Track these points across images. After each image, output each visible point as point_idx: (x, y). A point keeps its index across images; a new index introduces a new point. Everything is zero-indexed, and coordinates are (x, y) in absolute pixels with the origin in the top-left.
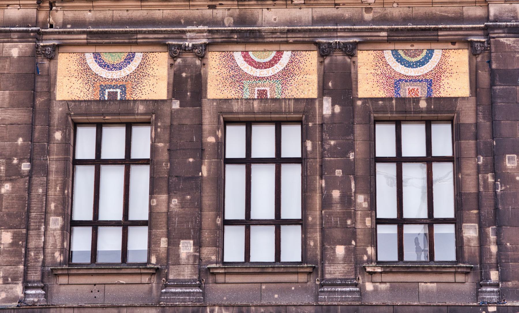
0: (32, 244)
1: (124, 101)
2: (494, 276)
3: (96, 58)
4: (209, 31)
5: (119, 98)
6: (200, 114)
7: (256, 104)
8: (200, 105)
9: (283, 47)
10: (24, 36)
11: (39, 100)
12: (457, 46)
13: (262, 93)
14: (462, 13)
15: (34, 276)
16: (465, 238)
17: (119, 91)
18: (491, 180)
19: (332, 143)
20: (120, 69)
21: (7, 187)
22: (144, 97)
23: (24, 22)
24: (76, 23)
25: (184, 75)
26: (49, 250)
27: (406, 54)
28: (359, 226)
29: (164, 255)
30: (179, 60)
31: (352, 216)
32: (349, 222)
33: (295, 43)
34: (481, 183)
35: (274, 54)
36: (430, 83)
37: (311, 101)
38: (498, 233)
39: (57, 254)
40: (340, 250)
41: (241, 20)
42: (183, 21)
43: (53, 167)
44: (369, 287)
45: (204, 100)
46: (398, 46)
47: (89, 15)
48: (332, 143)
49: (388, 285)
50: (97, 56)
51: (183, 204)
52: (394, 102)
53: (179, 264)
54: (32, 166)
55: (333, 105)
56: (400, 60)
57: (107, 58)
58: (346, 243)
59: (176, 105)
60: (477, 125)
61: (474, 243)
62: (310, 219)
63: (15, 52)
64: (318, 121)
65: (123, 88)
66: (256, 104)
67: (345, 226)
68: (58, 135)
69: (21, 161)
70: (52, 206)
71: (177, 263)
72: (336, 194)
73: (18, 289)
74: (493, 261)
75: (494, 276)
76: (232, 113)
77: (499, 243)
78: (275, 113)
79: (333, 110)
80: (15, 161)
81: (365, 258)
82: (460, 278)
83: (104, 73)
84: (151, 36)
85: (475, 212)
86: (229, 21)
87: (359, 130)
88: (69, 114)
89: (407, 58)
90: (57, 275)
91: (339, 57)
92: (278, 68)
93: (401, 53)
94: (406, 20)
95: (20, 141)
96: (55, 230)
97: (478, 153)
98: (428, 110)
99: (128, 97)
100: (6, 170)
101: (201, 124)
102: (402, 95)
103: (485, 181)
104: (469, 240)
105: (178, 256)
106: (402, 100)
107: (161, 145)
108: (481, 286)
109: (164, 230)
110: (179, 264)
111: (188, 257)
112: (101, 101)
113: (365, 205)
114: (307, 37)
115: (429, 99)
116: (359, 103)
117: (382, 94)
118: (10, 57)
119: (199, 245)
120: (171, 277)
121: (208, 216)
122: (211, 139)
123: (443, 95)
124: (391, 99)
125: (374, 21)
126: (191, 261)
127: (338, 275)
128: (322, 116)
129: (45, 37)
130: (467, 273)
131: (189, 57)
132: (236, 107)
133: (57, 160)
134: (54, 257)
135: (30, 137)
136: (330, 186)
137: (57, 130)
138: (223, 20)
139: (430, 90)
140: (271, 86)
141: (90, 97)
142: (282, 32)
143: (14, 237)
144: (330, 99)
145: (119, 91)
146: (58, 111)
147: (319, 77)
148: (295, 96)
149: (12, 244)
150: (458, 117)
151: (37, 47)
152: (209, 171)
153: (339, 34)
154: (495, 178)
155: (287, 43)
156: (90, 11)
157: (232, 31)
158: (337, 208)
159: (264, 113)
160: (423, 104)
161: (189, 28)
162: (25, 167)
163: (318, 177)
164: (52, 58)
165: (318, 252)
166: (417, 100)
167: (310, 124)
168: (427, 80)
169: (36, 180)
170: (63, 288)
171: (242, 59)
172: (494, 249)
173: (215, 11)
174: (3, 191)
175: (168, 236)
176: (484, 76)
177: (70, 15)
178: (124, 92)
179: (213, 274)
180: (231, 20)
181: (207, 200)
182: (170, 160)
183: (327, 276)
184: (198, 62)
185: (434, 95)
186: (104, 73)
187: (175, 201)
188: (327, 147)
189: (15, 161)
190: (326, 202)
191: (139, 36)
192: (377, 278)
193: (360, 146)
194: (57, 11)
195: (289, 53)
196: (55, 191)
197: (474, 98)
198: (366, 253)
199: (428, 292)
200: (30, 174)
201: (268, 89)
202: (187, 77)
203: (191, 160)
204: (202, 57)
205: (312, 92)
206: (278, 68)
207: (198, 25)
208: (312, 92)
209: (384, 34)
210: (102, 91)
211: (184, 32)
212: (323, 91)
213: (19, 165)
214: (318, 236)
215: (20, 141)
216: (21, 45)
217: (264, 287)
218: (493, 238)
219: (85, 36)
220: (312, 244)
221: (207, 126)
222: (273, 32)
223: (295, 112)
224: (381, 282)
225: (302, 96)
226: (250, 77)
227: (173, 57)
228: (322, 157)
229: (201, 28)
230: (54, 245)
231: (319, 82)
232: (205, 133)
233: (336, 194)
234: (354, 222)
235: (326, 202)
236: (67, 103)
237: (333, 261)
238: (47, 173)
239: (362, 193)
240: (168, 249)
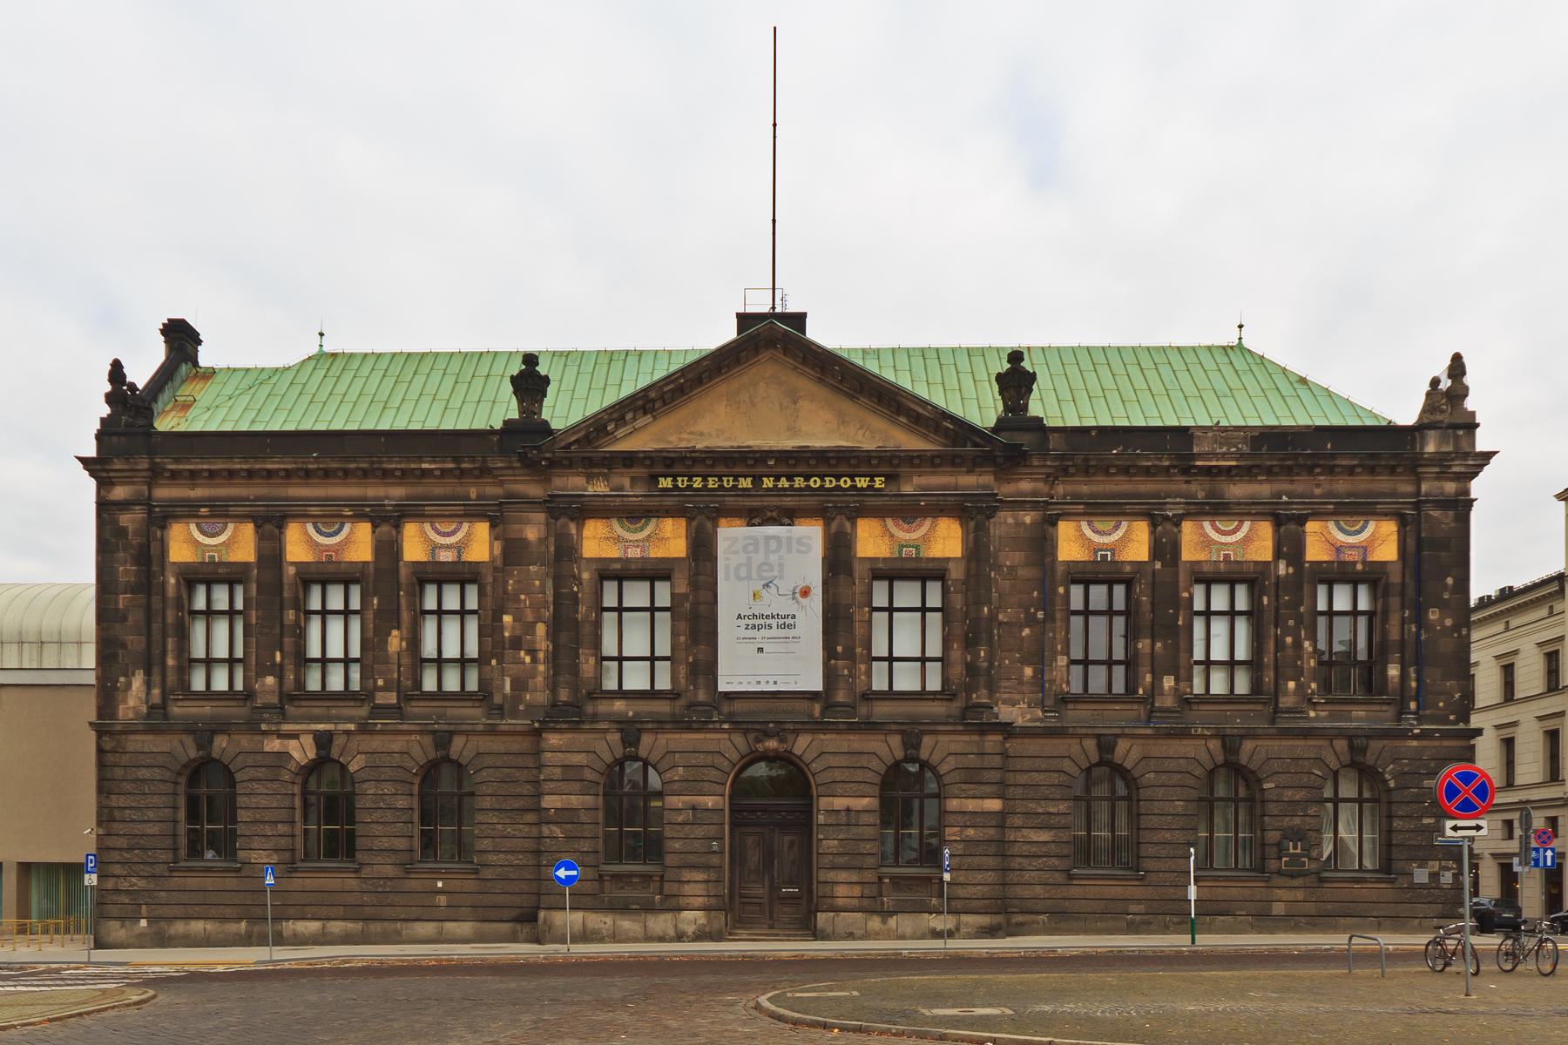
0: (1046, 678)
1: (1113, 562)
2: (1413, 705)
3: (1089, 525)
4: (1186, 503)
5: (1109, 559)
6: (1176, 574)
7: (1222, 565)
8: (1177, 566)
9: (1245, 518)
10: (1035, 506)
11: (1048, 560)
12: (1388, 518)
13: (1227, 556)
14: (1396, 489)
15: (1049, 702)
16: (1389, 677)
17: (1109, 553)
18: (1414, 629)
19: (1286, 598)
20: (1110, 534)
21: (1026, 632)
22: (1129, 559)
23: (1035, 493)
24: (1075, 495)
25: (1164, 540)
26: (1058, 682)
27: (1346, 524)
28: (1305, 666)
29: (1149, 688)
30: (1160, 528)
31: (1300, 657)
32: (1299, 663)
33: (1256, 514)
34: (1406, 631)
35: (1236, 523)
36: (1365, 549)
37: (1266, 563)
38: (1418, 672)
39: (1064, 686)
40: (1292, 685)
41: (1211, 494)
42: (1163, 495)
43: (1058, 616)
44: (1312, 714)
45: (1180, 563)
46: (1338, 518)
47: (1085, 489)
48: (1286, 598)
49: (1326, 713)
50: (1090, 524)
51: (1165, 646)
52: (1336, 564)
53: (1162, 694)
54: (1045, 615)
55: (1287, 566)
56: (1341, 530)
57: (1099, 526)
58: (1296, 679)
59: (1158, 565)
60: (1403, 583)
61: (1396, 680)
62: (1266, 660)
63: (1028, 520)
64: (1273, 580)
65: (1113, 551)
66: (1222, 565)
67: (1297, 666)
68: (1061, 590)
69: (1037, 610)
70: (1059, 647)
71: (1162, 694)
72: (1289, 640)
73: (1040, 714)
74: (1413, 693)
75: (1413, 705)
76: (1202, 573)
77: (1418, 680)
78: (1238, 573)
79: (1287, 571)
80: (1032, 610)
81: (1310, 691)
82: (1385, 708)
83: (1097, 539)
84: (1137, 507)
85: (1398, 655)
86: (1201, 494)
87: (1306, 588)
88: (1069, 573)
89: (1347, 528)
90: (1066, 702)
91: (1292, 527)
92: (1240, 535)
93: (1341, 523)
94: (1349, 495)
95: (1035, 593)
96: (1063, 666)
97: (1403, 608)
98: (1363, 572)
99: (1117, 558)
100: (1025, 617)
101: (1178, 582)
102: (1342, 559)
103: (1410, 630)
104: (1392, 677)
105: (1162, 687)
106: (1342, 563)
107: (1144, 598)
108: (1403, 714)
109: (1149, 668)
110: (1162, 694)
111: (1170, 690)
112: (1095, 562)
113: (1310, 649)
114: (1266, 509)
115: (1364, 562)
116: (1307, 565)
117: (1325, 558)
118: (1025, 524)
119: (1177, 680)
120: (1157, 705)
121: (1183, 656)
122: (1186, 595)
123: (1375, 559)
124: (1333, 562)
125: (1321, 496)
126: (1173, 692)
127: (1289, 705)
128: (1278, 577)
129: (1050, 507)
130: (1389, 704)
131: (1168, 526)
132: (1206, 568)
133: (1061, 610)
134: (1061, 687)
135: (1042, 591)
136: (1286, 633)
137: (1061, 586)
138: (1196, 494)
139: (1364, 558)
140: (1233, 550)
141: (1086, 558)
142: (1246, 504)
143: (1034, 672)
144: (1285, 562)
145: (1109, 553)
146: (1060, 569)
147: (1274, 541)
148: (1254, 559)
149: (1033, 677)
150: (1388, 577)
151: (1045, 515)
152: (1183, 620)
153: (1294, 506)
154: (1419, 628)
155: (1249, 514)
156: (1085, 485)
157: (1207, 503)
158: (1290, 652)
159: (1229, 573)
160: (1359, 567)
161: (1168, 500)
162: (1040, 615)
163: (1272, 627)
164: (1054, 524)
165: (1272, 686)
166: (1355, 563)
167: (1267, 583)
168: (1363, 547)
169: (1048, 626)
170: (1069, 712)
171: (1210, 527)
172: (1414, 684)
173: (1190, 486)
174: (1024, 634)
175: (1153, 672)
176: (1411, 542)
177: (1069, 488)
178: (1113, 555)
179: (1190, 703)
180: (1203, 494)
181: (1183, 645)
182: (1153, 612)
183: (1281, 705)
184: (1175, 530)
185: (1370, 559)
186: (1097, 539)
187: (1159, 645)
188: (1282, 601)
189: (1032, 610)
190: (1279, 645)
191: (1128, 507)
192: (1319, 707)
193: (1306, 600)
194: (1058, 484)
195: (1249, 523)
196: (1060, 635)
197: (1401, 562)
198: (1310, 687)
199: (1358, 719)
200: (1044, 621)
201: (1231, 553)
202: (1166, 543)
203: (1171, 611)
204: (1178, 525)
205: (1267, 556)
206: (1240, 535)
207: (1176, 497)
208: (1267, 556)
209: (1332, 507)
210: (1096, 553)
211: (1166, 503)
212: (1278, 554)
213: (1035, 614)
214: (1272, 674)
215: (1035, 593)
216: (1032, 513)
217: (1228, 713)
218: (1413, 675)
219: (1082, 507)
220: (1267, 680)
221: (1181, 584)
222: (1239, 504)
223: (1255, 572)
224: (1322, 711)
225: (1259, 559)
226: (1217, 543)
227: (1154, 525)
228: (1277, 609)
229: (1178, 500)
230: (1062, 679)
231: (1273, 546)
232: (1181, 589)
233: (1289, 640)
234: (1302, 663)
235: (1279, 645)
236: (1068, 563)
237: (1286, 693)
238: (1053, 620)
239: (1307, 640)
240: (1153, 683)
